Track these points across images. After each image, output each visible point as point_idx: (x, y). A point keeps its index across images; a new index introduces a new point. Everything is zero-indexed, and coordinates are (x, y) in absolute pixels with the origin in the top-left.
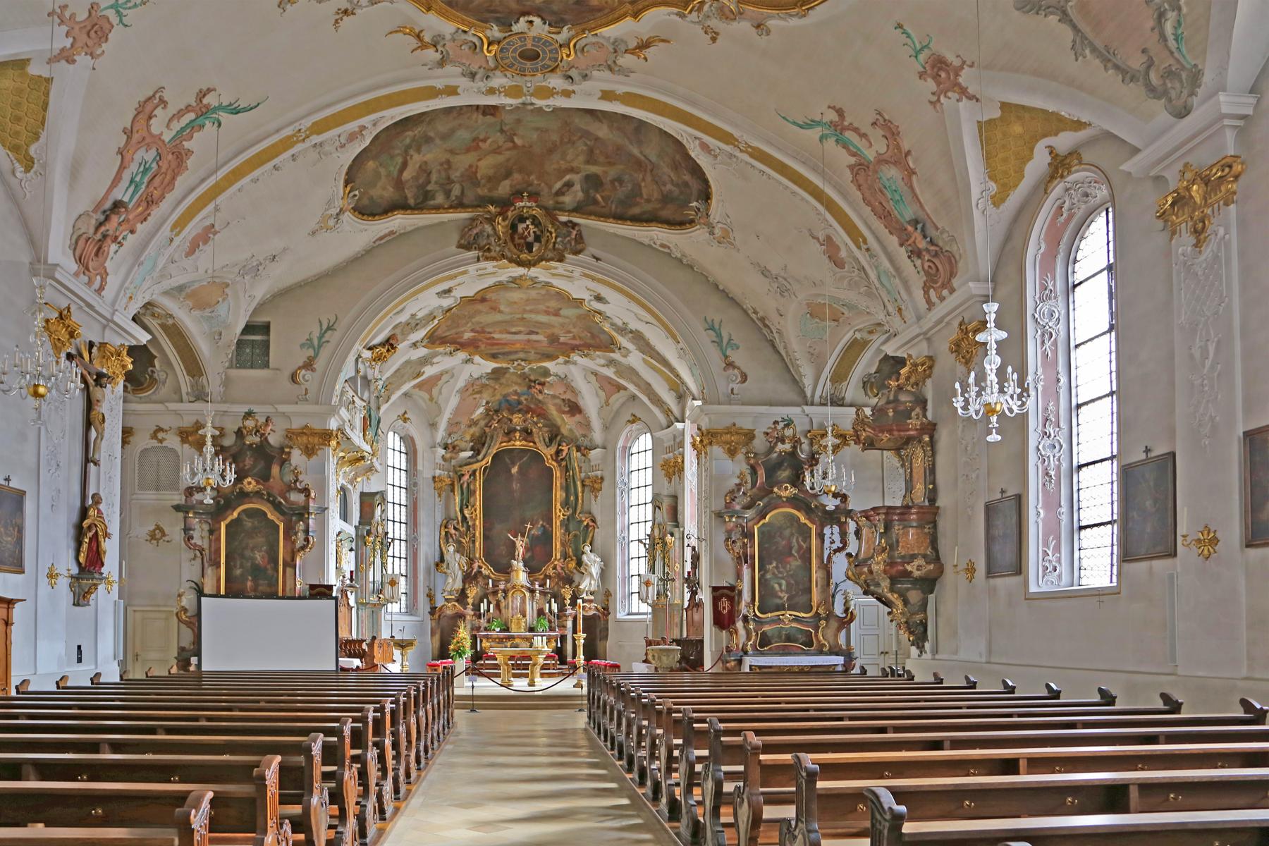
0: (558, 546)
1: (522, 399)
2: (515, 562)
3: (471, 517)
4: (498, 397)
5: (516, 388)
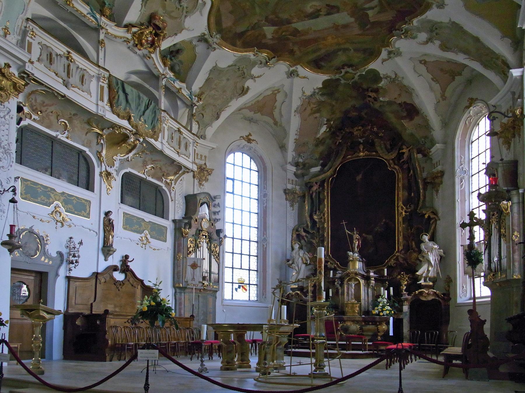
0: (401, 240)
1: (363, 114)
2: (351, 253)
3: (320, 222)
4: (338, 115)
5: (353, 102)
